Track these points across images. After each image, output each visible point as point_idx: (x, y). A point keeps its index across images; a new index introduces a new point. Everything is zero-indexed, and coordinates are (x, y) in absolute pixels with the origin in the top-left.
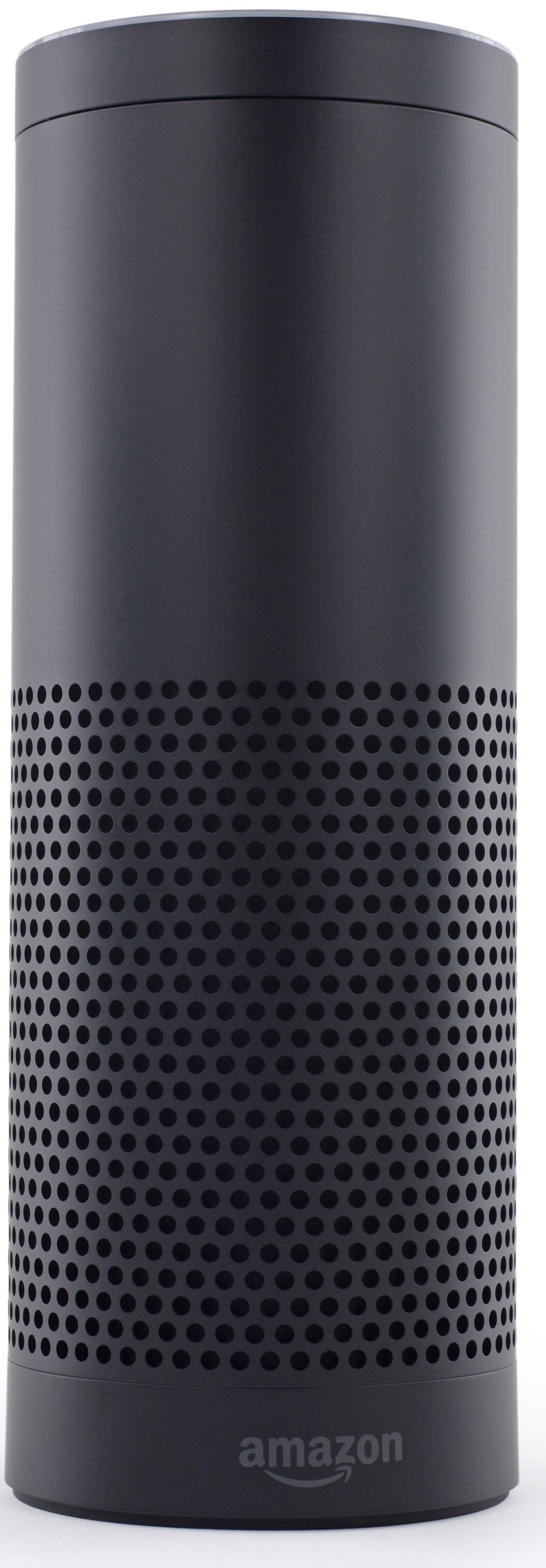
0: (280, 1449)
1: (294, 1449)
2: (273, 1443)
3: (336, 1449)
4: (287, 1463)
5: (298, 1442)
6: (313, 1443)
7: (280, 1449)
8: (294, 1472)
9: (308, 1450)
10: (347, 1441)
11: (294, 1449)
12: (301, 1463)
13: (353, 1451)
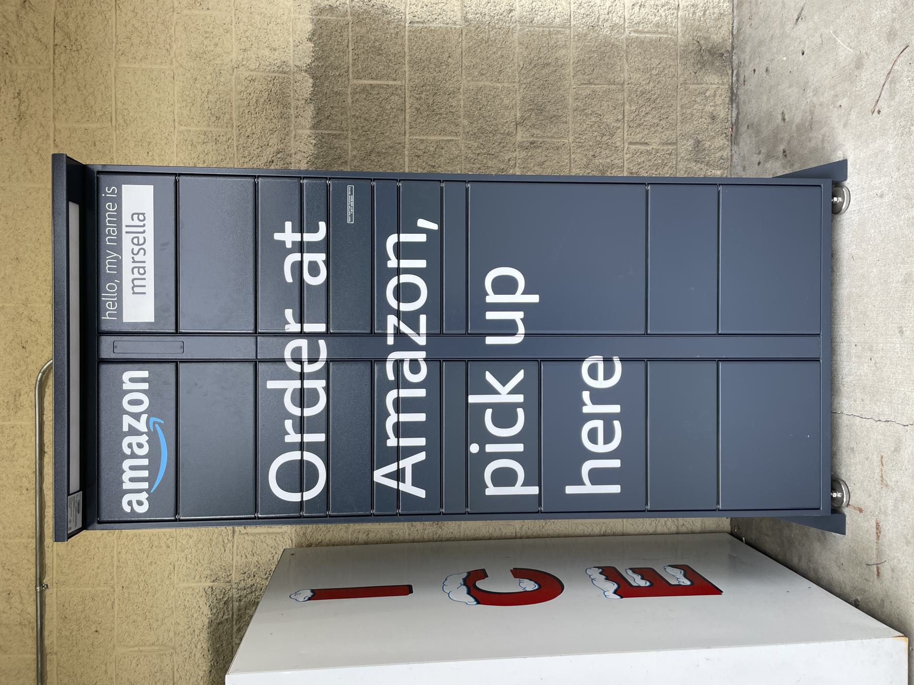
0: (132, 480)
1: (132, 468)
2: (127, 485)
3: (133, 432)
4: (145, 474)
5: (126, 464)
6: (128, 451)
7: (132, 480)
8: (153, 468)
9: (134, 456)
10: (127, 421)
11: (132, 468)
12: (145, 462)
13: (137, 416)
